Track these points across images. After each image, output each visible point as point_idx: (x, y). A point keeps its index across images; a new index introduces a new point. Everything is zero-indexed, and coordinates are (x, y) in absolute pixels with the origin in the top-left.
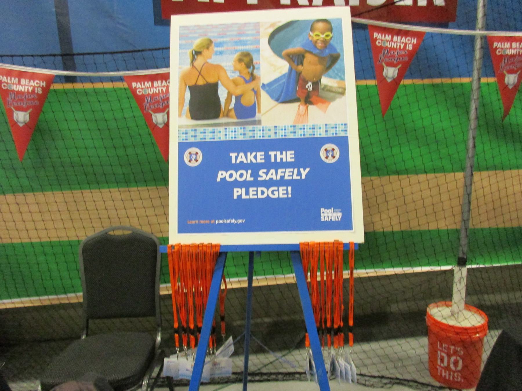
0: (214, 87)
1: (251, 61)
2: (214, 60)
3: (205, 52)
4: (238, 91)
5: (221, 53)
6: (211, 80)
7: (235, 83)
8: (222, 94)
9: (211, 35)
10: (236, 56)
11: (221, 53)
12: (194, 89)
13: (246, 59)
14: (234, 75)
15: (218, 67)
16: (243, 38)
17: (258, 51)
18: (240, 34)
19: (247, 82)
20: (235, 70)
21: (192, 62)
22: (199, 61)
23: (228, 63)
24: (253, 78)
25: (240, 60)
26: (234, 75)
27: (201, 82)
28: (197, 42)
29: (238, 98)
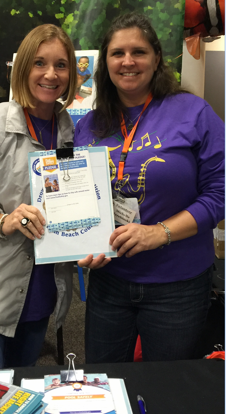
0: (50, 187)
1: (56, 181)
2: (49, 182)
3: (48, 180)
4: (55, 187)
5: (51, 180)
6: (49, 186)
7: (54, 186)
8: (52, 188)
9: (48, 177)
10: (53, 181)
11: (51, 180)
12: (46, 188)
13: (56, 181)
14: (54, 184)
15: (50, 183)
16: (54, 177)
17: (58, 179)
18: (53, 176)
19: (56, 185)
20: (54, 183)
21: (45, 183)
22: (47, 182)
23: (52, 182)
24: (57, 185)
25: (54, 181)
26: (54, 184)
27: (48, 186)
28: (46, 178)
29: (55, 189)
